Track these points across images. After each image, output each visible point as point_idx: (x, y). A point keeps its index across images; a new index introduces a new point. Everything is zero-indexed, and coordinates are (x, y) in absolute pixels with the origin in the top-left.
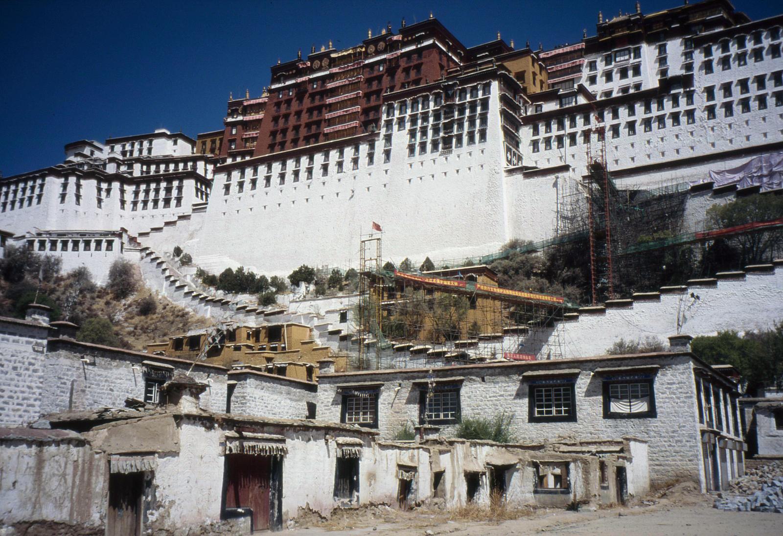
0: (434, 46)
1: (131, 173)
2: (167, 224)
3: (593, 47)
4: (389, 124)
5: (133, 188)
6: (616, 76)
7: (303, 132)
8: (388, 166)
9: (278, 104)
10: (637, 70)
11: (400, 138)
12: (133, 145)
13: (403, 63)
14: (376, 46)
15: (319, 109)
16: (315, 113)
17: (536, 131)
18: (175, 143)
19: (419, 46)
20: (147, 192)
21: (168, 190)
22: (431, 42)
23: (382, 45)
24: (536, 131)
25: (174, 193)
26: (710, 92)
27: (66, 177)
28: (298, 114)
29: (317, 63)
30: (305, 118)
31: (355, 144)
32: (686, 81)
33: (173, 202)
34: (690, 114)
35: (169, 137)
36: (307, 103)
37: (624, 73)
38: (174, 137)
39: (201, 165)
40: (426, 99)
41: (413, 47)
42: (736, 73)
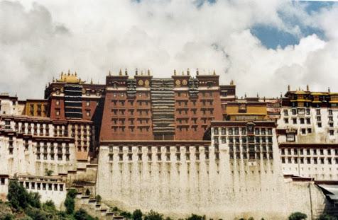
1: (9, 128)
2: (69, 172)
4: (216, 138)
5: (35, 144)
11: (224, 146)
13: (201, 97)
14: (181, 82)
17: (283, 153)
19: (210, 89)
20: (45, 148)
21: (60, 149)
22: (217, 88)
23: (185, 82)
25: (64, 151)
27: (11, 137)
29: (141, 82)
30: (136, 115)
31: (197, 145)
33: (64, 157)
36: (136, 105)
37: (302, 121)
39: (51, 127)
40: (237, 129)
41: (205, 88)
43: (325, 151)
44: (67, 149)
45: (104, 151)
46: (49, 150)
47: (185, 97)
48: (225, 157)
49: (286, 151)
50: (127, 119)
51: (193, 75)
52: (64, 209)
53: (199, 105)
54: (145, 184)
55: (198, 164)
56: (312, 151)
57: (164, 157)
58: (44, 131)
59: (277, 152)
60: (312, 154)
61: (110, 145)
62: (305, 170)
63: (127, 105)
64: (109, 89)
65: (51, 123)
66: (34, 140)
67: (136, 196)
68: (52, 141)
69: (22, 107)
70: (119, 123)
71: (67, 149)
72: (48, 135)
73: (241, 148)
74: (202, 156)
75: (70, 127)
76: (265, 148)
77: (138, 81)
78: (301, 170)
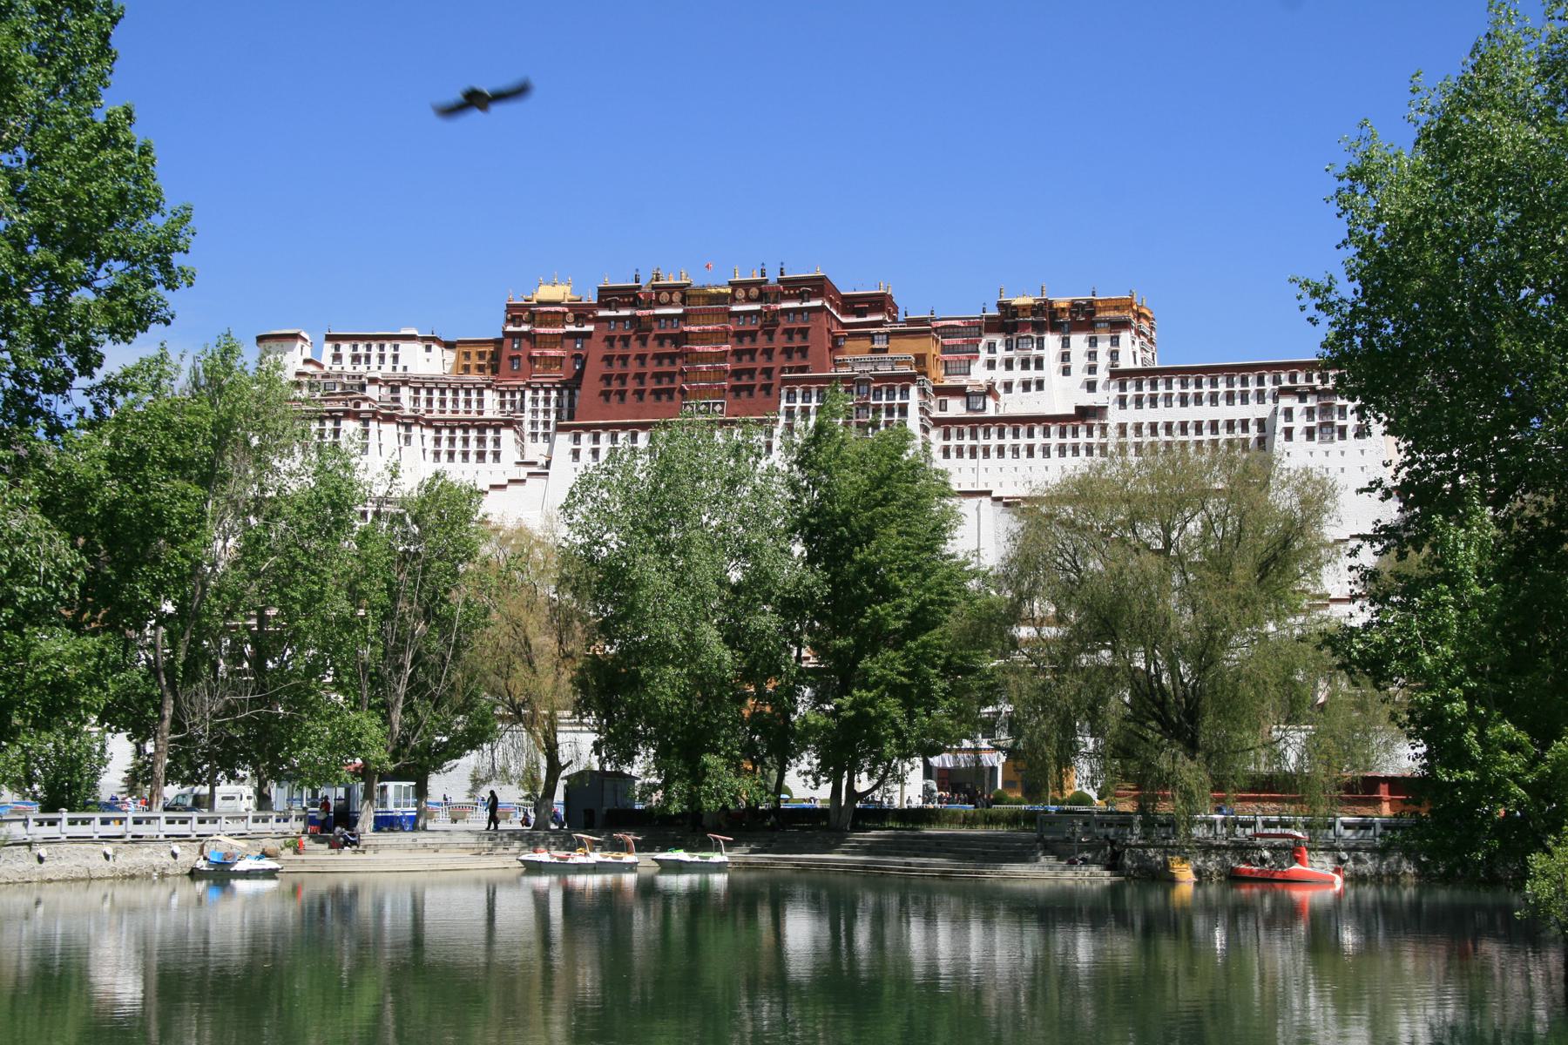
0: (822, 308)
1: (397, 400)
2: (493, 487)
3: (992, 325)
5: (430, 433)
6: (1017, 367)
7: (651, 385)
9: (610, 340)
10: (1039, 364)
12: (369, 347)
13: (784, 323)
14: (747, 291)
15: (672, 357)
16: (666, 361)
18: (428, 349)
19: (805, 304)
20: (452, 441)
21: (481, 441)
22: (817, 303)
23: (754, 292)
24: (947, 436)
25: (490, 446)
26: (1122, 428)
28: (641, 358)
29: (664, 296)
33: (489, 457)
35: (424, 339)
38: (429, 341)
39: (488, 394)
42: (1147, 415)
46: (459, 445)
47: (753, 325)
50: (631, 375)
51: (773, 277)
53: (780, 341)
56: (1037, 430)
58: (474, 405)
60: (1009, 440)
63: (635, 348)
64: (602, 313)
65: (489, 386)
66: (429, 424)
69: (450, 356)
70: (615, 386)
72: (480, 413)
75: (529, 394)
77: (658, 294)
78: (982, 471)
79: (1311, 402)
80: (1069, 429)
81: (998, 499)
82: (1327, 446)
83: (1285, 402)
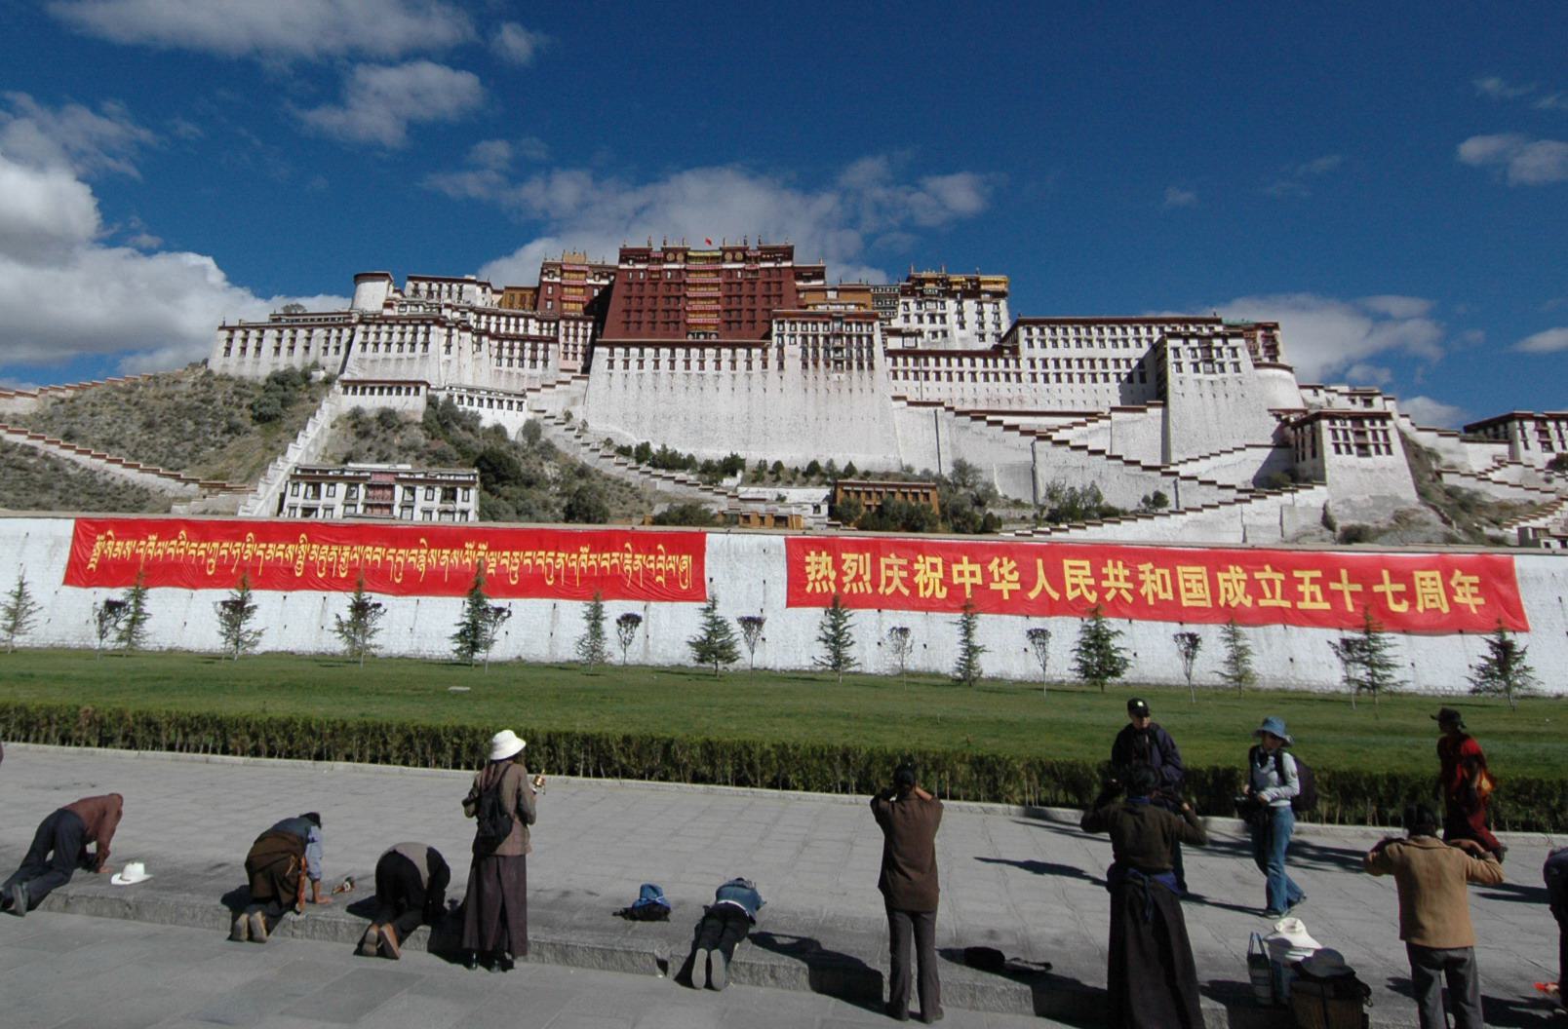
5: (496, 343)
8: (785, 374)
11: (793, 350)
17: (895, 363)
21: (534, 350)
25: (540, 354)
31: (749, 347)
32: (1015, 351)
33: (540, 364)
34: (1018, 375)
42: (1050, 352)
43: (966, 361)
44: (546, 350)
45: (601, 352)
48: (793, 363)
49: (900, 360)
52: (521, 440)
54: (663, 407)
55: (750, 377)
57: (695, 365)
59: (883, 364)
61: (611, 346)
62: (933, 390)
66: (493, 337)
67: (646, 424)
68: (523, 339)
71: (546, 350)
73: (821, 351)
74: (757, 364)
76: (860, 349)
79: (1194, 343)
80: (990, 362)
81: (949, 409)
82: (1212, 377)
83: (1171, 343)
